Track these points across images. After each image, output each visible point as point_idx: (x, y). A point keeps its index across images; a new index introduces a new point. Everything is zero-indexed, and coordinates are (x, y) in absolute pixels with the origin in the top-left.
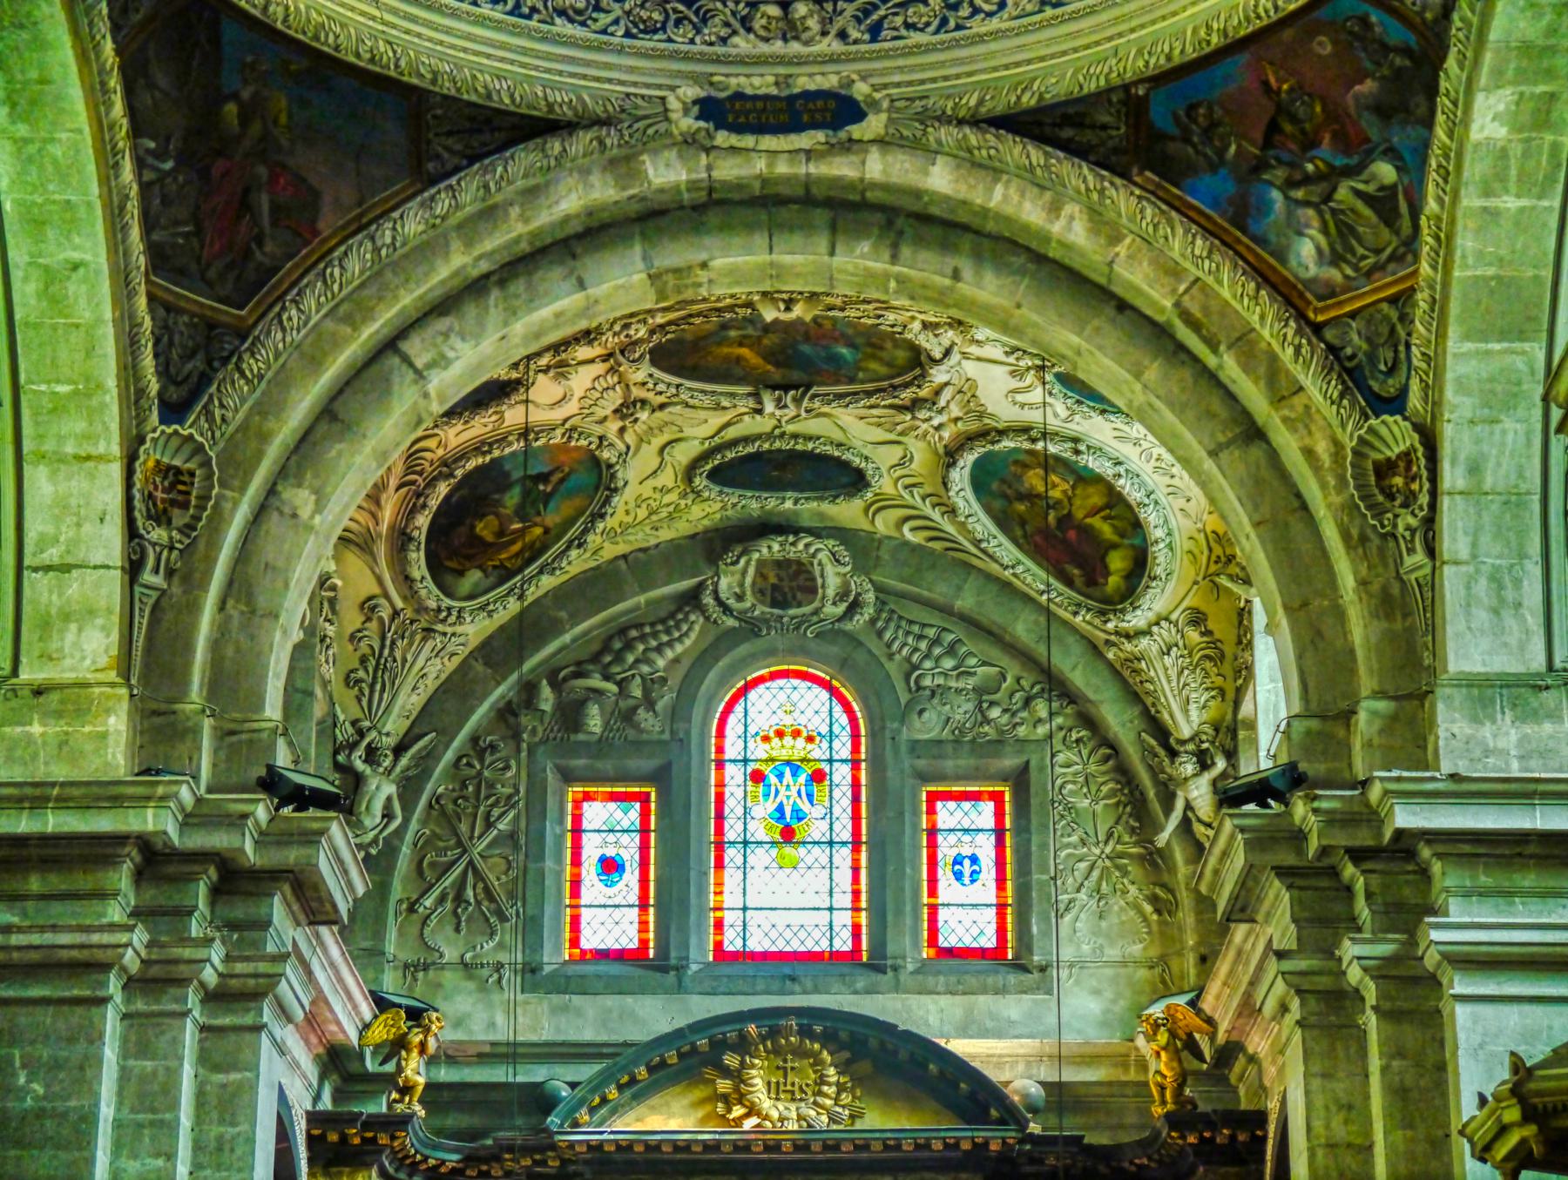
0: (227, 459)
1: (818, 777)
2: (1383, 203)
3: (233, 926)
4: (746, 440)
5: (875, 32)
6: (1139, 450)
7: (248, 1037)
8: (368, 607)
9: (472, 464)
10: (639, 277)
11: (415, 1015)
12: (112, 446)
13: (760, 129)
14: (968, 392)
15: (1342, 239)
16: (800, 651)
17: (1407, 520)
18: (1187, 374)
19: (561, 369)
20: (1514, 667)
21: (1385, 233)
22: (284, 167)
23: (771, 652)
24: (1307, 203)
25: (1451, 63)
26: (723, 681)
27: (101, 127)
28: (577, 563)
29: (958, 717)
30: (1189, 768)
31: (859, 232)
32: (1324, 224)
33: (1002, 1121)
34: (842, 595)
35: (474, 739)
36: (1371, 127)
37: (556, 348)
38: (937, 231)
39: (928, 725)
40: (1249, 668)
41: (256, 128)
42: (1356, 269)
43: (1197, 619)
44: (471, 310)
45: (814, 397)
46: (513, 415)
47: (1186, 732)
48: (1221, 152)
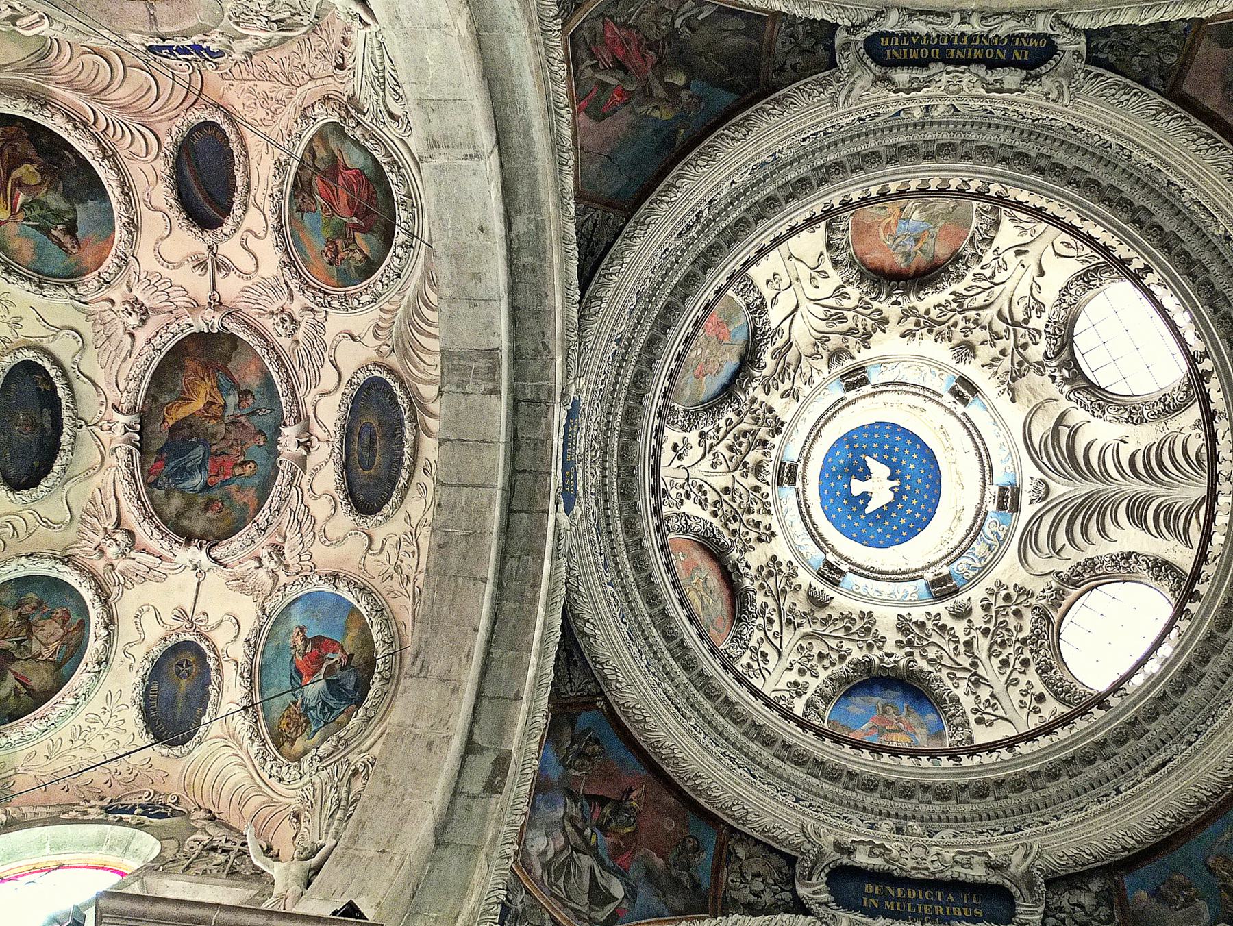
6: (99, 711)
15: (560, 868)
22: (625, 104)
24: (566, 837)
32: (561, 852)
42: (550, 884)
45: (130, 452)
48: (571, 766)
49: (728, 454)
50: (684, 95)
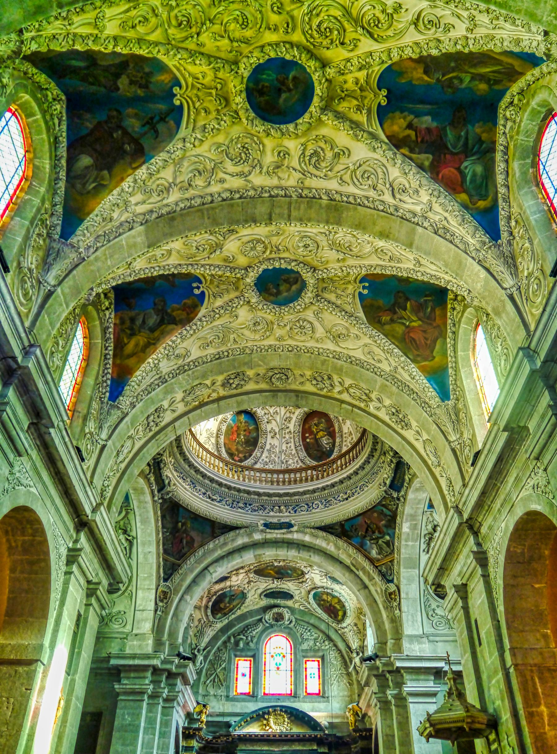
0: (175, 590)
1: (284, 656)
2: (387, 543)
3: (170, 685)
4: (271, 589)
5: (295, 512)
7: (171, 709)
8: (200, 621)
9: (220, 593)
10: (252, 556)
11: (204, 706)
12: (154, 587)
13: (275, 529)
14: (312, 580)
15: (380, 549)
16: (281, 631)
17: (395, 604)
18: (353, 575)
19: (237, 574)
20: (417, 633)
21: (388, 549)
23: (275, 631)
25: (398, 518)
26: (266, 637)
27: (157, 527)
28: (239, 613)
29: (311, 644)
30: (355, 655)
31: (292, 548)
33: (320, 730)
34: (289, 620)
35: (218, 648)
36: (385, 530)
37: (237, 570)
38: (307, 548)
39: (305, 646)
40: (366, 635)
41: (184, 528)
43: (356, 625)
44: (221, 562)
46: (228, 583)
47: (354, 648)
49: (273, 408)
50: (183, 521)
